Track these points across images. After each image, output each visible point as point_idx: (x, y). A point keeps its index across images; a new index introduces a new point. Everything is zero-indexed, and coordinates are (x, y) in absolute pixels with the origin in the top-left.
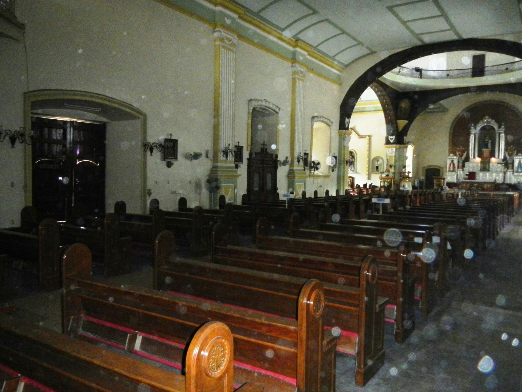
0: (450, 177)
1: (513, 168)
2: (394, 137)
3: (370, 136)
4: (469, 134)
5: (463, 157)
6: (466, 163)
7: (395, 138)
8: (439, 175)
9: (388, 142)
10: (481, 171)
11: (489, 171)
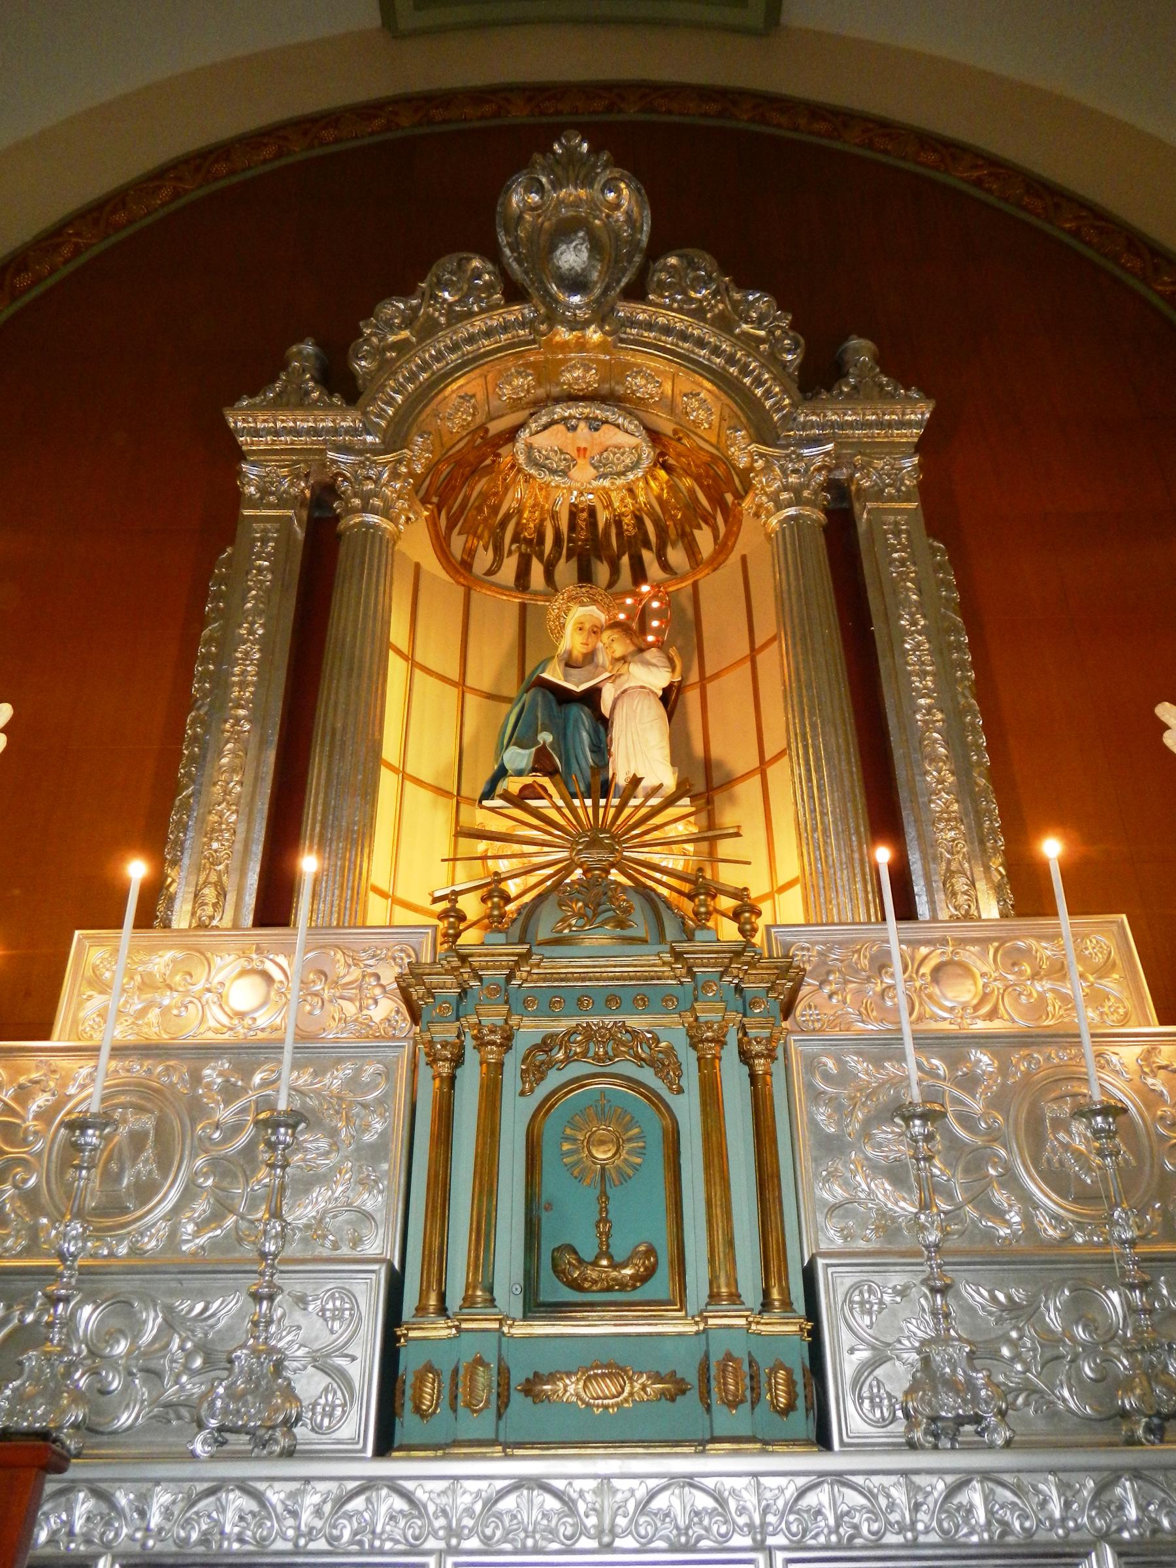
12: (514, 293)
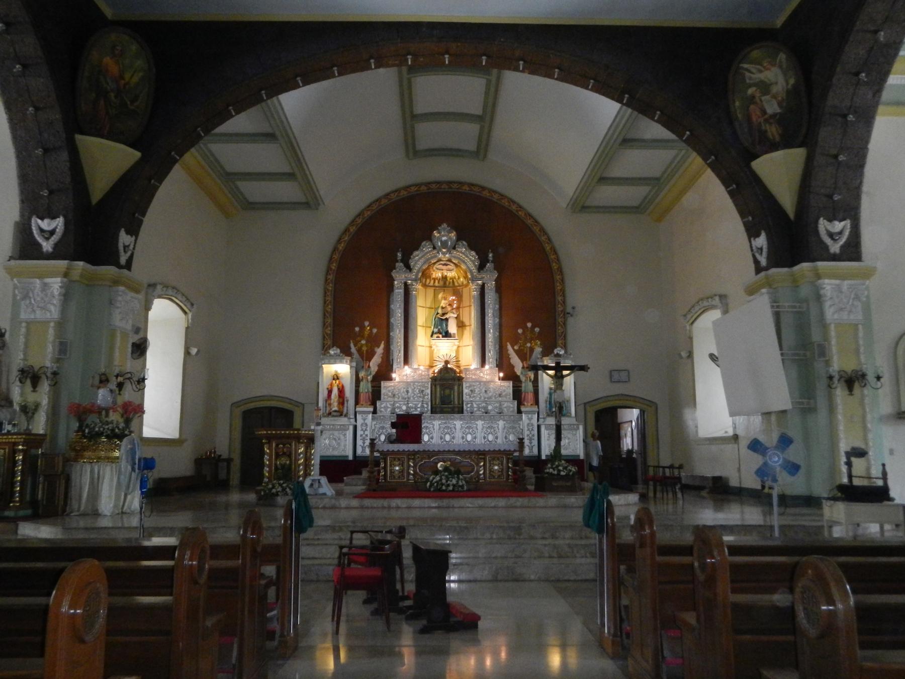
0: (335, 440)
1: (537, 402)
2: (58, 223)
4: (390, 288)
5: (374, 364)
6: (384, 384)
7: (66, 224)
8: (289, 424)
9: (26, 248)
10: (434, 411)
11: (461, 411)
12: (434, 248)
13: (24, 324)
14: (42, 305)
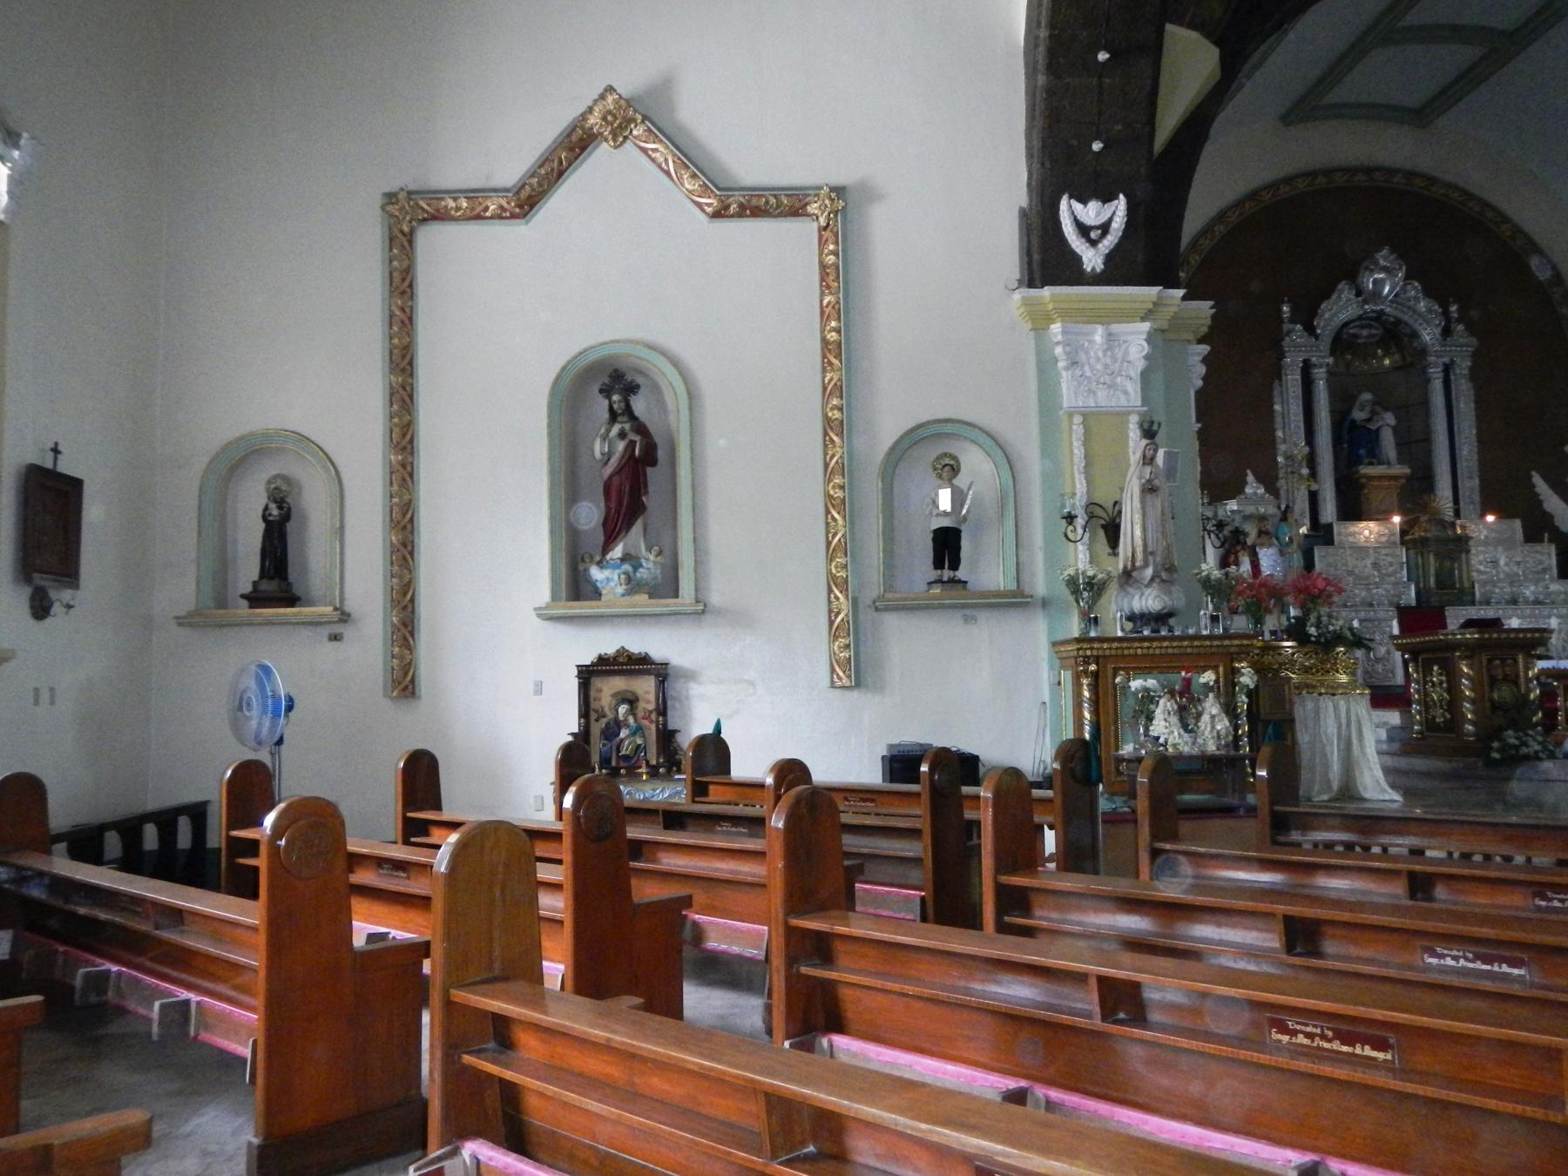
3: (836, 212)
4: (1277, 373)
13: (1078, 419)
14: (1108, 379)
